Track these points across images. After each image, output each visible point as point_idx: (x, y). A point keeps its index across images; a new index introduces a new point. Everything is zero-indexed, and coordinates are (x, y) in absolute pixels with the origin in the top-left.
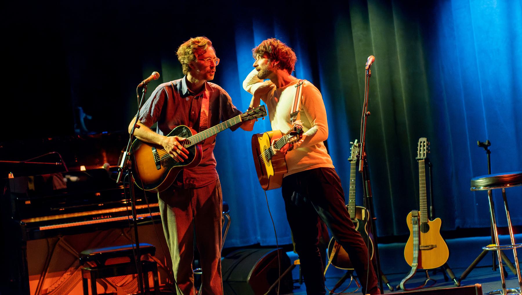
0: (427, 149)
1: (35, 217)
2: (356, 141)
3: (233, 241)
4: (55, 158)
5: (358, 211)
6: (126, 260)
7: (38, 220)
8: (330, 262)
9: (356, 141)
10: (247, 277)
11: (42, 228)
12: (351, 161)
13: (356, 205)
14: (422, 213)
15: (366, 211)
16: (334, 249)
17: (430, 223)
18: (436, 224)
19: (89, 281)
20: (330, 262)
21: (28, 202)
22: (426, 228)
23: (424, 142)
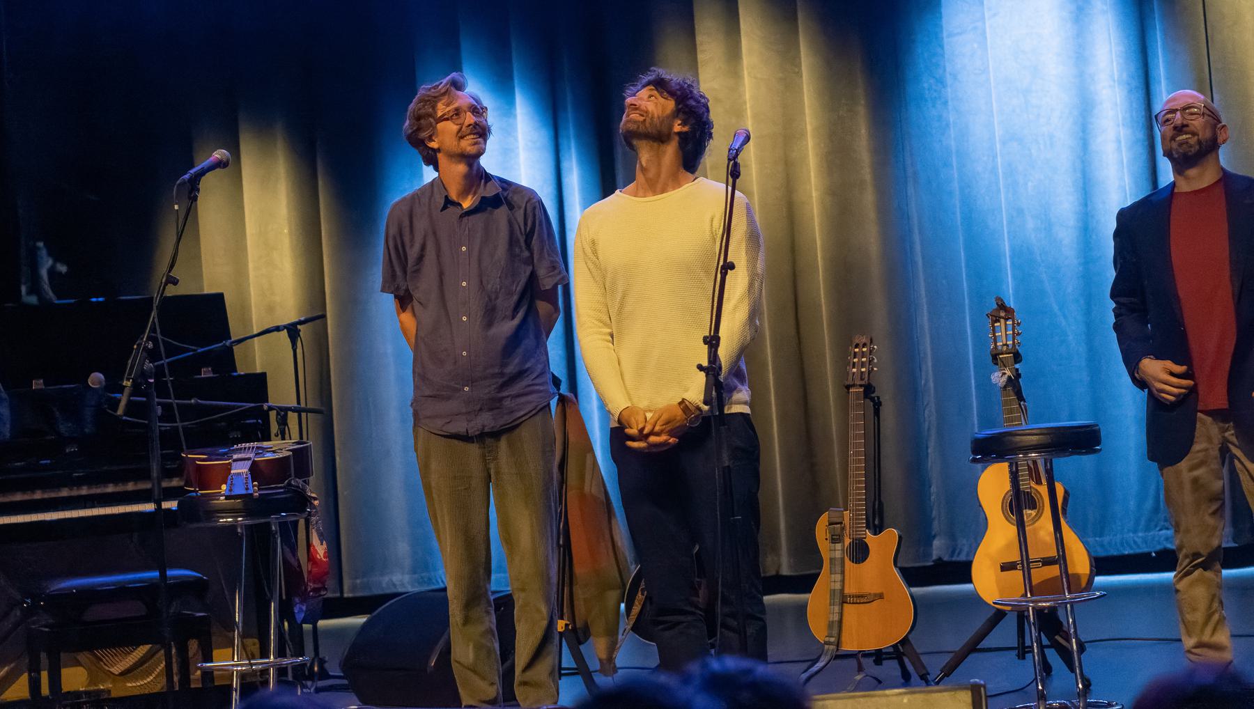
0: (870, 361)
3: (397, 578)
6: (135, 609)
10: (428, 658)
14: (851, 516)
16: (640, 597)
17: (870, 538)
18: (883, 545)
19: (43, 656)
22: (860, 552)
23: (864, 345)
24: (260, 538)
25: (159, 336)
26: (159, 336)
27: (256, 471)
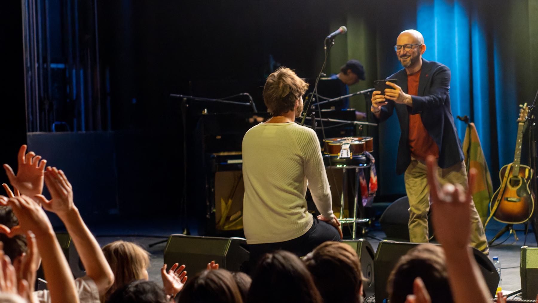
1: (224, 151)
2: (526, 104)
4: (247, 99)
5: (522, 170)
7: (226, 154)
8: (491, 215)
9: (526, 104)
11: (230, 162)
12: (520, 122)
13: (521, 163)
15: (529, 170)
20: (491, 215)
21: (219, 137)
24: (351, 173)
25: (317, 95)
26: (317, 95)
27: (352, 148)
